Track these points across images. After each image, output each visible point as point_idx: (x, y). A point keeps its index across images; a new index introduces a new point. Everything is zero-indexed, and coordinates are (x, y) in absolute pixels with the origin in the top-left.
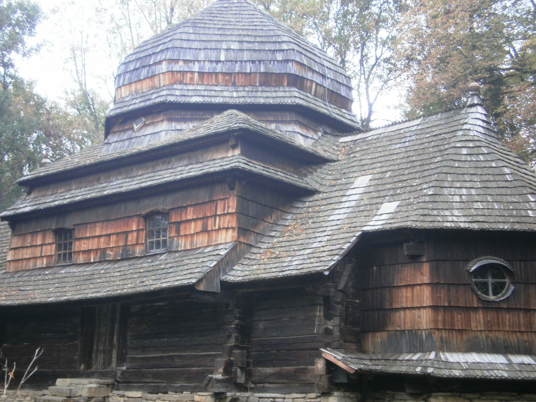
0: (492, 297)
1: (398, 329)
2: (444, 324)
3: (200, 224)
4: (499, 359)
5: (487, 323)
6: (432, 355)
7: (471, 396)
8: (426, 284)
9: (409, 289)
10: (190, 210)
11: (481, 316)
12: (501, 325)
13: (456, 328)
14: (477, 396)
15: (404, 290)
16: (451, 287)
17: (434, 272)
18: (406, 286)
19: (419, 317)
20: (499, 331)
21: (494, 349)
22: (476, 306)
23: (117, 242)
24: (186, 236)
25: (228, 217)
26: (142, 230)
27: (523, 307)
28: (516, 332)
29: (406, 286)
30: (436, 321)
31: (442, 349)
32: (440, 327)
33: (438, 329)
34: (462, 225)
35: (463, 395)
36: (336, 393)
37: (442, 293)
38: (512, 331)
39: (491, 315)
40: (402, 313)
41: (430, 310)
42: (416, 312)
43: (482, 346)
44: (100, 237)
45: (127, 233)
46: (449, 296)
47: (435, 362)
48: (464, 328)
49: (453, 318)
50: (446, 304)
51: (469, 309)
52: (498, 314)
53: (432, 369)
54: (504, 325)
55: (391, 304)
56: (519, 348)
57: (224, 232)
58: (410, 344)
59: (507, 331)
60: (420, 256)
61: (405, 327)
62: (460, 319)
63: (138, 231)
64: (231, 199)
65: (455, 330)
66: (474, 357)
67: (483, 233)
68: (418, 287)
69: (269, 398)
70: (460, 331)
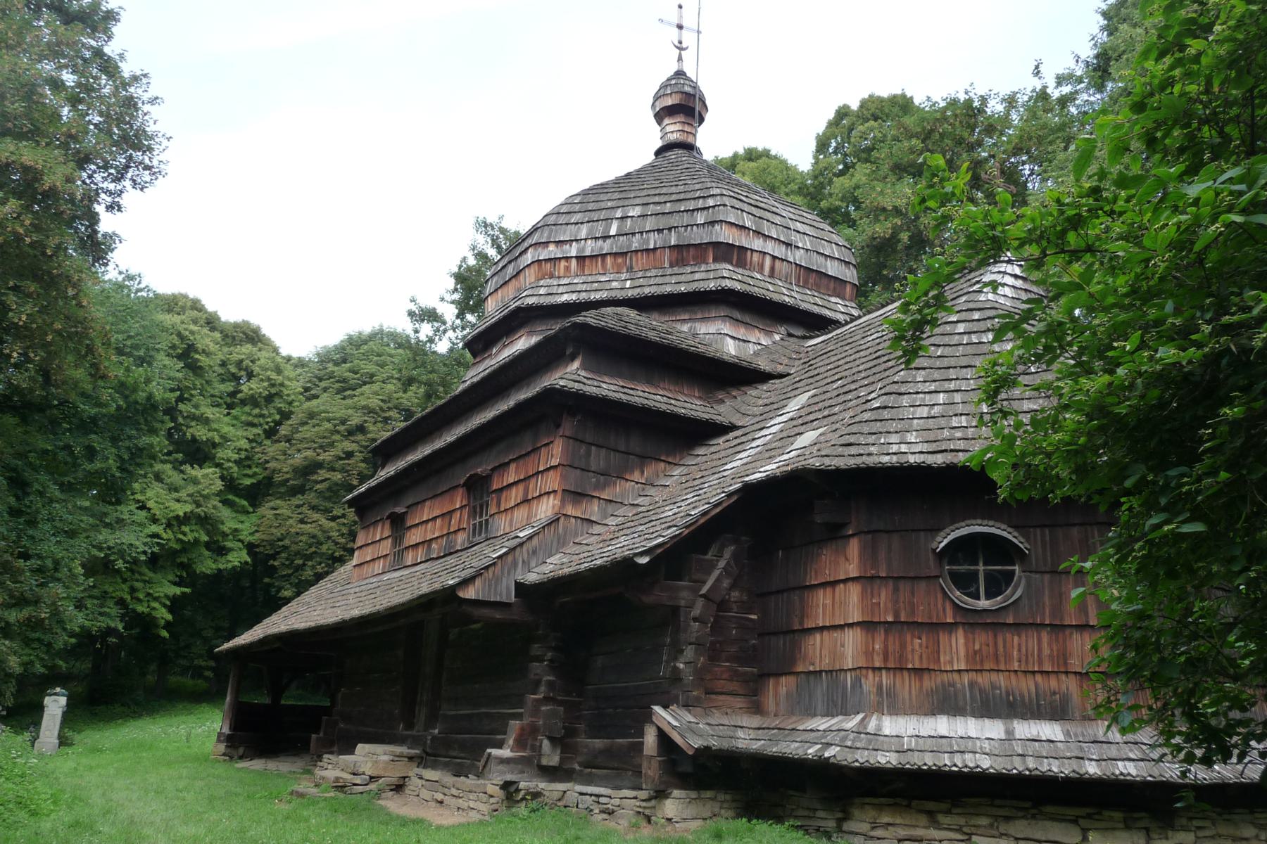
0: (983, 603)
1: (811, 668)
2: (886, 659)
3: (521, 487)
4: (993, 729)
5: (972, 656)
6: (852, 722)
7: (931, 805)
8: (853, 579)
9: (829, 590)
10: (513, 466)
11: (961, 641)
12: (1002, 659)
13: (910, 666)
14: (944, 806)
15: (821, 592)
16: (901, 584)
17: (869, 554)
18: (824, 585)
19: (843, 646)
20: (998, 671)
21: (987, 708)
22: (950, 620)
23: (441, 528)
24: (506, 510)
25: (551, 473)
26: (465, 506)
27: (1047, 622)
28: (1034, 672)
29: (824, 585)
30: (869, 654)
31: (879, 709)
32: (877, 665)
33: (874, 669)
34: (912, 459)
35: (914, 803)
36: (676, 793)
37: (884, 596)
38: (1025, 672)
39: (981, 639)
40: (818, 636)
41: (859, 630)
42: (836, 634)
43: (961, 703)
44: (427, 521)
45: (451, 512)
46: (896, 602)
47: (852, 736)
48: (925, 666)
49: (903, 646)
50: (890, 619)
51: (935, 627)
52: (995, 636)
53: (838, 748)
54: (1008, 658)
55: (801, 623)
56: (1039, 705)
57: (545, 498)
58: (828, 700)
59: (1016, 671)
60: (844, 525)
61: (820, 666)
62: (917, 647)
63: (462, 507)
64: (556, 443)
65: (909, 669)
66: (942, 725)
67: (950, 470)
68: (842, 585)
69: (591, 795)
70: (918, 672)
